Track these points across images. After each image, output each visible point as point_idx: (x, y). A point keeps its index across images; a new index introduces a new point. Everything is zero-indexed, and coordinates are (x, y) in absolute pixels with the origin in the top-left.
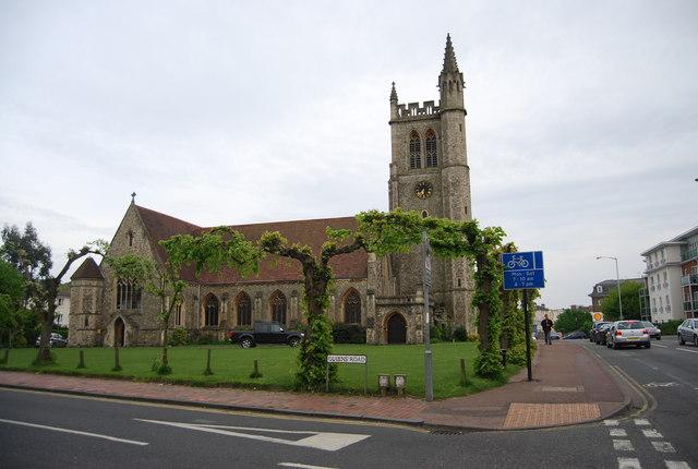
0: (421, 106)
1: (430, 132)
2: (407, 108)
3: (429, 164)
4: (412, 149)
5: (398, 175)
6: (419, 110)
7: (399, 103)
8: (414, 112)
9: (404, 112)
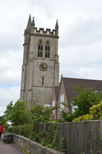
0: (45, 30)
1: (48, 42)
2: (38, 29)
3: (46, 56)
4: (39, 46)
5: (33, 59)
6: (44, 32)
7: (35, 27)
8: (41, 32)
9: (37, 31)
